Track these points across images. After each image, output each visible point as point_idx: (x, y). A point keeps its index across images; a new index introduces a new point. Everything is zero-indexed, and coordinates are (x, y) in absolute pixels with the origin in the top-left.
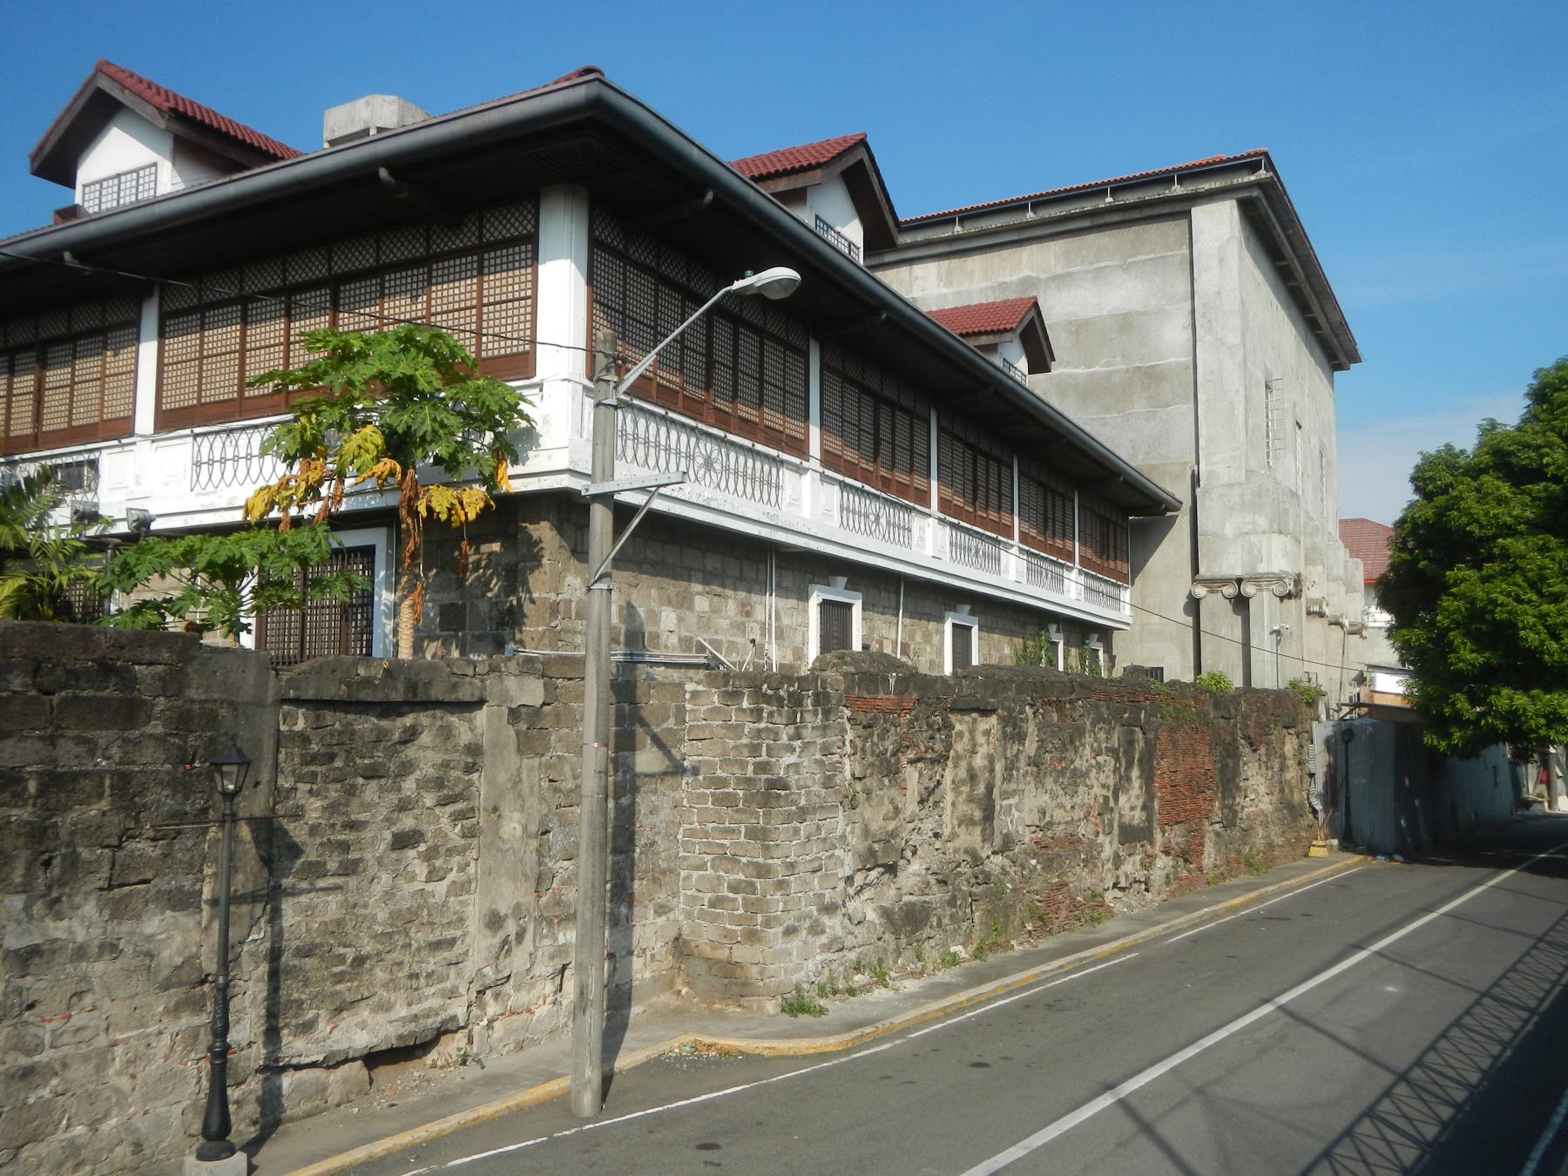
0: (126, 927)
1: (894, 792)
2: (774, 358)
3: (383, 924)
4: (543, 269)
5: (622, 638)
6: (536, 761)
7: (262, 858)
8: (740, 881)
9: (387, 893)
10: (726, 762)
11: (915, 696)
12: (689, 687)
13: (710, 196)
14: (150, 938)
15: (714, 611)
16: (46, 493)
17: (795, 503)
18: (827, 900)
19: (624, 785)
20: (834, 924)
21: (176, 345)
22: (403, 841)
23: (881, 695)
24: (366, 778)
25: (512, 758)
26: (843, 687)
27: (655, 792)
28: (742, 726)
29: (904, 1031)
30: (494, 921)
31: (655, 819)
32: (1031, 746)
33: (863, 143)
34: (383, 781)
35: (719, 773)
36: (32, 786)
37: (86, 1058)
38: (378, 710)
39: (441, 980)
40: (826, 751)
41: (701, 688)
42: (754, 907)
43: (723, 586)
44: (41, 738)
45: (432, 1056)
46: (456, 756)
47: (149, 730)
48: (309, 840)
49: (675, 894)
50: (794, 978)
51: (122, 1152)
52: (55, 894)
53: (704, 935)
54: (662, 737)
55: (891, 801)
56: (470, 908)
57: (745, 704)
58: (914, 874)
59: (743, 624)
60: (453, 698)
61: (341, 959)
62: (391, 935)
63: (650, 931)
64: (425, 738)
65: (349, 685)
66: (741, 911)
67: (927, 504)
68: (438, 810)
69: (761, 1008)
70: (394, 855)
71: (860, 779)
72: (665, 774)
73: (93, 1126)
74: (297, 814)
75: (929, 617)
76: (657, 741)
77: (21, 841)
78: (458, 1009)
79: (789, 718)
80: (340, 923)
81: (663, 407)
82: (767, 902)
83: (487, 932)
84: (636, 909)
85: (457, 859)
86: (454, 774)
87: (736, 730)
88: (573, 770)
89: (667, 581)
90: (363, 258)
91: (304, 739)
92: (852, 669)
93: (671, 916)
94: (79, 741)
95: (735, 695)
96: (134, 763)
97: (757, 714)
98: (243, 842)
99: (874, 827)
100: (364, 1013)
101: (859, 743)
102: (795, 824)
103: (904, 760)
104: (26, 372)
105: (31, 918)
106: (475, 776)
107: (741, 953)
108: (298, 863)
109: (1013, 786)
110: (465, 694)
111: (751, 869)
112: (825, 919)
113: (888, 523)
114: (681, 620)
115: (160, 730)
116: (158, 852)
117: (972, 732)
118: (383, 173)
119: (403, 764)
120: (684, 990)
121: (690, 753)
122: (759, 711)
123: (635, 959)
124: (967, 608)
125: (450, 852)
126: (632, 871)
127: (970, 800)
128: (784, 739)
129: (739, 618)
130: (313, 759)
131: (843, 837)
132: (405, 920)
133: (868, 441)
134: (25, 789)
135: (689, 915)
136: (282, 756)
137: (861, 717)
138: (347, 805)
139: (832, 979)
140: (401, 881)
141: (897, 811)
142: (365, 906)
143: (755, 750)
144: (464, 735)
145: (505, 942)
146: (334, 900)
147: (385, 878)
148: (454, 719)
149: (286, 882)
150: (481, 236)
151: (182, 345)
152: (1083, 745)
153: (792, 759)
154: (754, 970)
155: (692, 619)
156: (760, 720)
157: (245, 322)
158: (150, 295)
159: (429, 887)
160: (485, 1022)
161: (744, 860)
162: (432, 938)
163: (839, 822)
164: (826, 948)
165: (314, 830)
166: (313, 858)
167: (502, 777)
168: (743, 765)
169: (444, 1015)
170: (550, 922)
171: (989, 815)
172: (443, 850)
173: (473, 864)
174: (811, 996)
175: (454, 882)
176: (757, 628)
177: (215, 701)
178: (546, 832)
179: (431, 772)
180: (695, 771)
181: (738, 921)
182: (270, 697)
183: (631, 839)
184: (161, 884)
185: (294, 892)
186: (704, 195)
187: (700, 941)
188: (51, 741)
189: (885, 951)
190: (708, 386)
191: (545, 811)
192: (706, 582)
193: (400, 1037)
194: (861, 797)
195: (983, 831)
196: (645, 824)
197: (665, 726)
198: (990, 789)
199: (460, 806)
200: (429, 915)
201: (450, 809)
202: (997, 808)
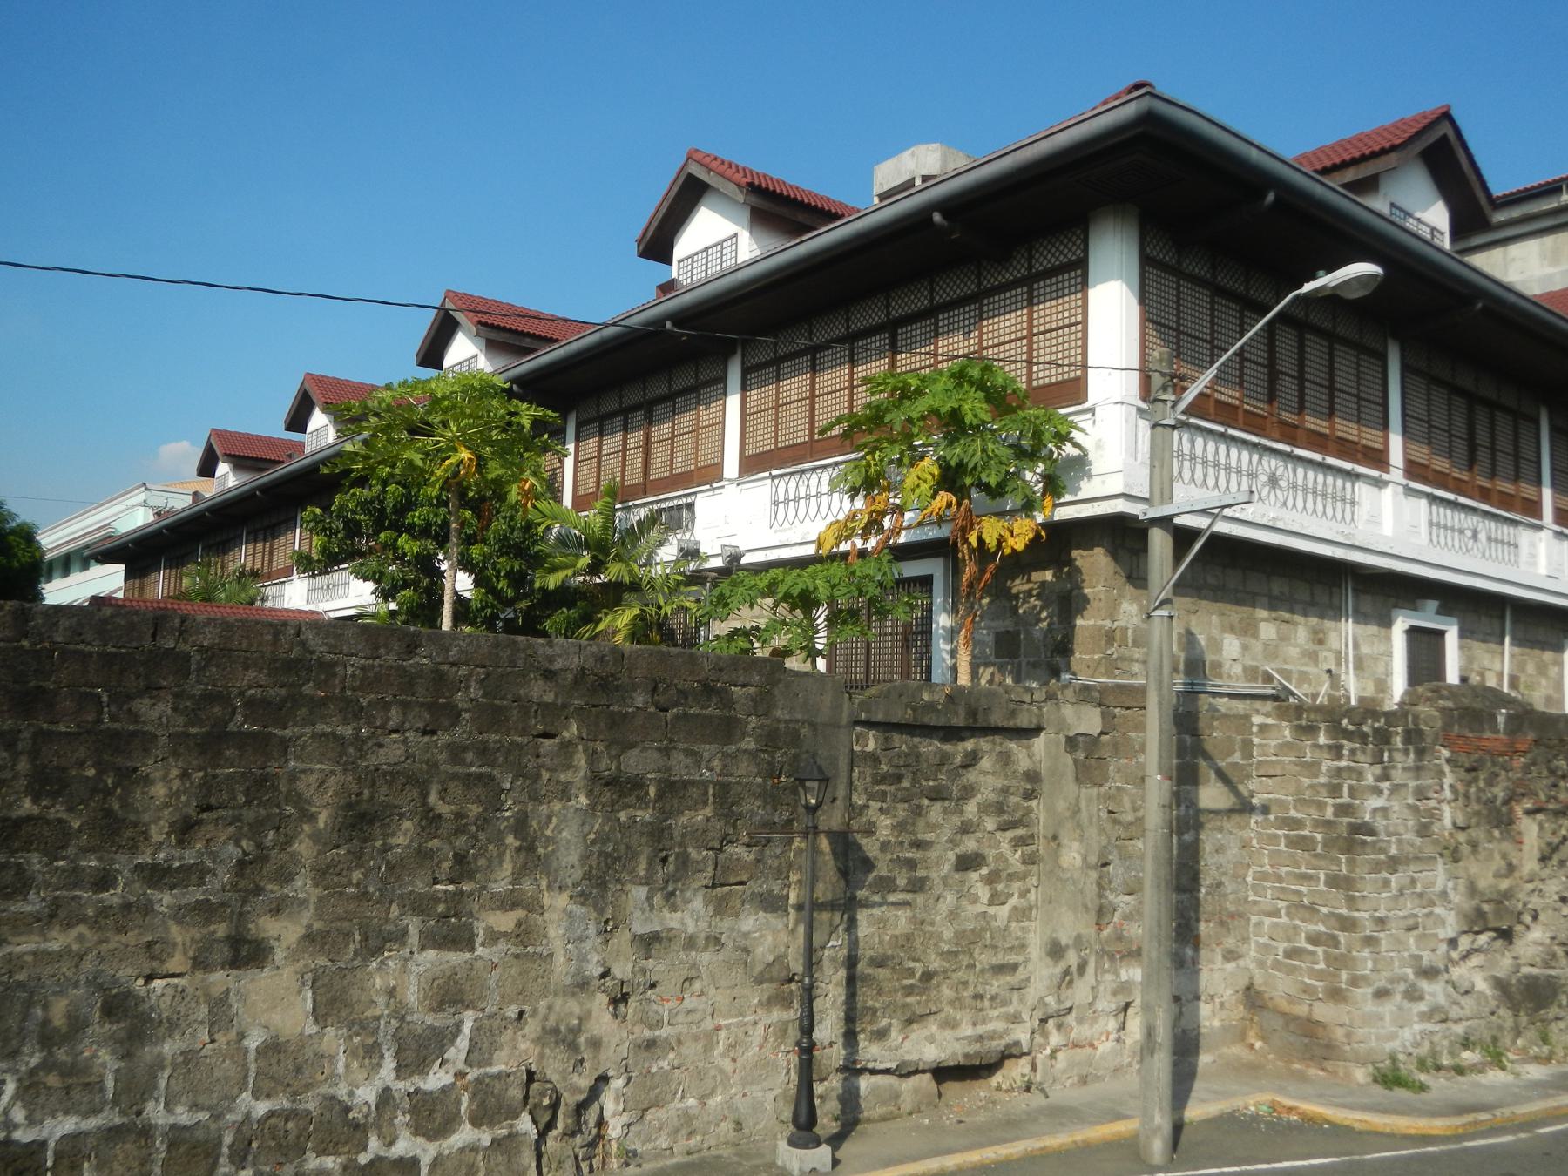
0: (726, 924)
2: (1345, 364)
3: (949, 942)
4: (1093, 294)
5: (1182, 667)
6: (1095, 791)
7: (839, 870)
8: (1319, 934)
9: (951, 912)
10: (1300, 802)
11: (1531, 736)
12: (1257, 720)
13: (1271, 197)
14: (746, 935)
16: (654, 534)
17: (1375, 519)
18: (1425, 962)
19: (1187, 822)
20: (1435, 991)
21: (756, 395)
22: (967, 863)
23: (1488, 734)
24: (932, 799)
25: (1070, 787)
26: (1439, 724)
27: (1221, 829)
28: (1319, 764)
29: (1530, 1124)
30: (1055, 951)
31: (1221, 859)
33: (1446, 116)
34: (947, 803)
35: (1293, 813)
36: (652, 791)
37: (696, 1038)
38: (941, 734)
39: (1005, 1003)
40: (1421, 794)
41: (1270, 721)
42: (1339, 962)
43: (1292, 612)
44: (659, 749)
45: (997, 1079)
46: (1015, 782)
47: (744, 745)
48: (880, 856)
49: (1245, 940)
50: (1389, 1046)
51: (726, 1127)
52: (670, 888)
53: (1280, 988)
54: (1229, 772)
55: (1504, 856)
56: (1032, 935)
57: (1322, 740)
58: (1536, 943)
60: (1011, 724)
61: (911, 973)
62: (956, 954)
63: (1218, 978)
64: (985, 763)
65: (914, 709)
66: (1322, 966)
67: (1540, 517)
68: (998, 835)
69: (1348, 1075)
70: (957, 876)
71: (1463, 829)
72: (1231, 811)
73: (702, 1100)
74: (870, 831)
75: (1544, 646)
76: (1222, 776)
77: (644, 840)
78: (1022, 1035)
79: (1374, 756)
80: (909, 937)
81: (1221, 424)
82: (1354, 959)
83: (1048, 960)
84: (1203, 953)
85: (1017, 885)
86: (1014, 800)
87: (1312, 768)
88: (1133, 802)
89: (1228, 606)
90: (918, 300)
91: (874, 759)
92: (1450, 704)
93: (1241, 963)
94: (689, 753)
95: (1310, 730)
96: (732, 775)
97: (1336, 752)
98: (822, 853)
99: (1482, 884)
100: (933, 1027)
101: (1460, 787)
102: (1385, 874)
103: (1518, 810)
104: (636, 429)
105: (652, 908)
106: (1034, 803)
107: (1324, 1012)
108: (872, 876)
110: (1023, 721)
111: (1333, 922)
112: (1424, 985)
113: (1489, 539)
114: (1245, 648)
115: (752, 746)
116: (752, 857)
118: (937, 217)
119: (965, 788)
120: (1258, 1044)
121: (1259, 790)
122: (1339, 748)
123: (1202, 1005)
125: (1012, 877)
126: (1197, 911)
128: (1369, 779)
129: (1311, 647)
130: (882, 779)
131: (1444, 894)
132: (969, 941)
133: (1461, 447)
134: (647, 793)
135: (1261, 964)
136: (855, 775)
137: (1464, 759)
138: (914, 824)
139: (1434, 1054)
140: (964, 903)
141: (1511, 868)
142: (932, 924)
143: (1335, 790)
144: (1023, 764)
145: (1067, 972)
146: (903, 915)
147: (950, 898)
148: (1013, 745)
149: (861, 894)
150: (1030, 267)
151: (762, 395)
153: (1375, 802)
154: (1339, 1034)
155: (1258, 647)
156: (1339, 757)
157: (814, 370)
158: (734, 353)
159: (992, 910)
160: (1048, 1051)
161: (1324, 910)
162: (994, 961)
163: (1439, 876)
164: (1426, 1017)
165: (885, 846)
166: (884, 873)
167: (1061, 805)
168: (1321, 806)
169: (1007, 1040)
170: (1112, 957)
172: (1004, 875)
173: (1033, 891)
174: (1408, 1068)
175: (1015, 908)
176: (1331, 656)
177: (797, 721)
178: (1106, 864)
179: (992, 797)
180: (1265, 810)
181: (1319, 975)
182: (845, 718)
183: (1195, 879)
184: (755, 886)
185: (868, 905)
186: (1264, 197)
187: (1274, 993)
188: (666, 752)
189: (1500, 1028)
190: (1271, 397)
191: (1104, 842)
192: (1272, 608)
193: (966, 1056)
194: (1465, 849)
196: (1210, 863)
197: (1230, 760)
199: (1020, 832)
200: (992, 938)
201: (1010, 834)
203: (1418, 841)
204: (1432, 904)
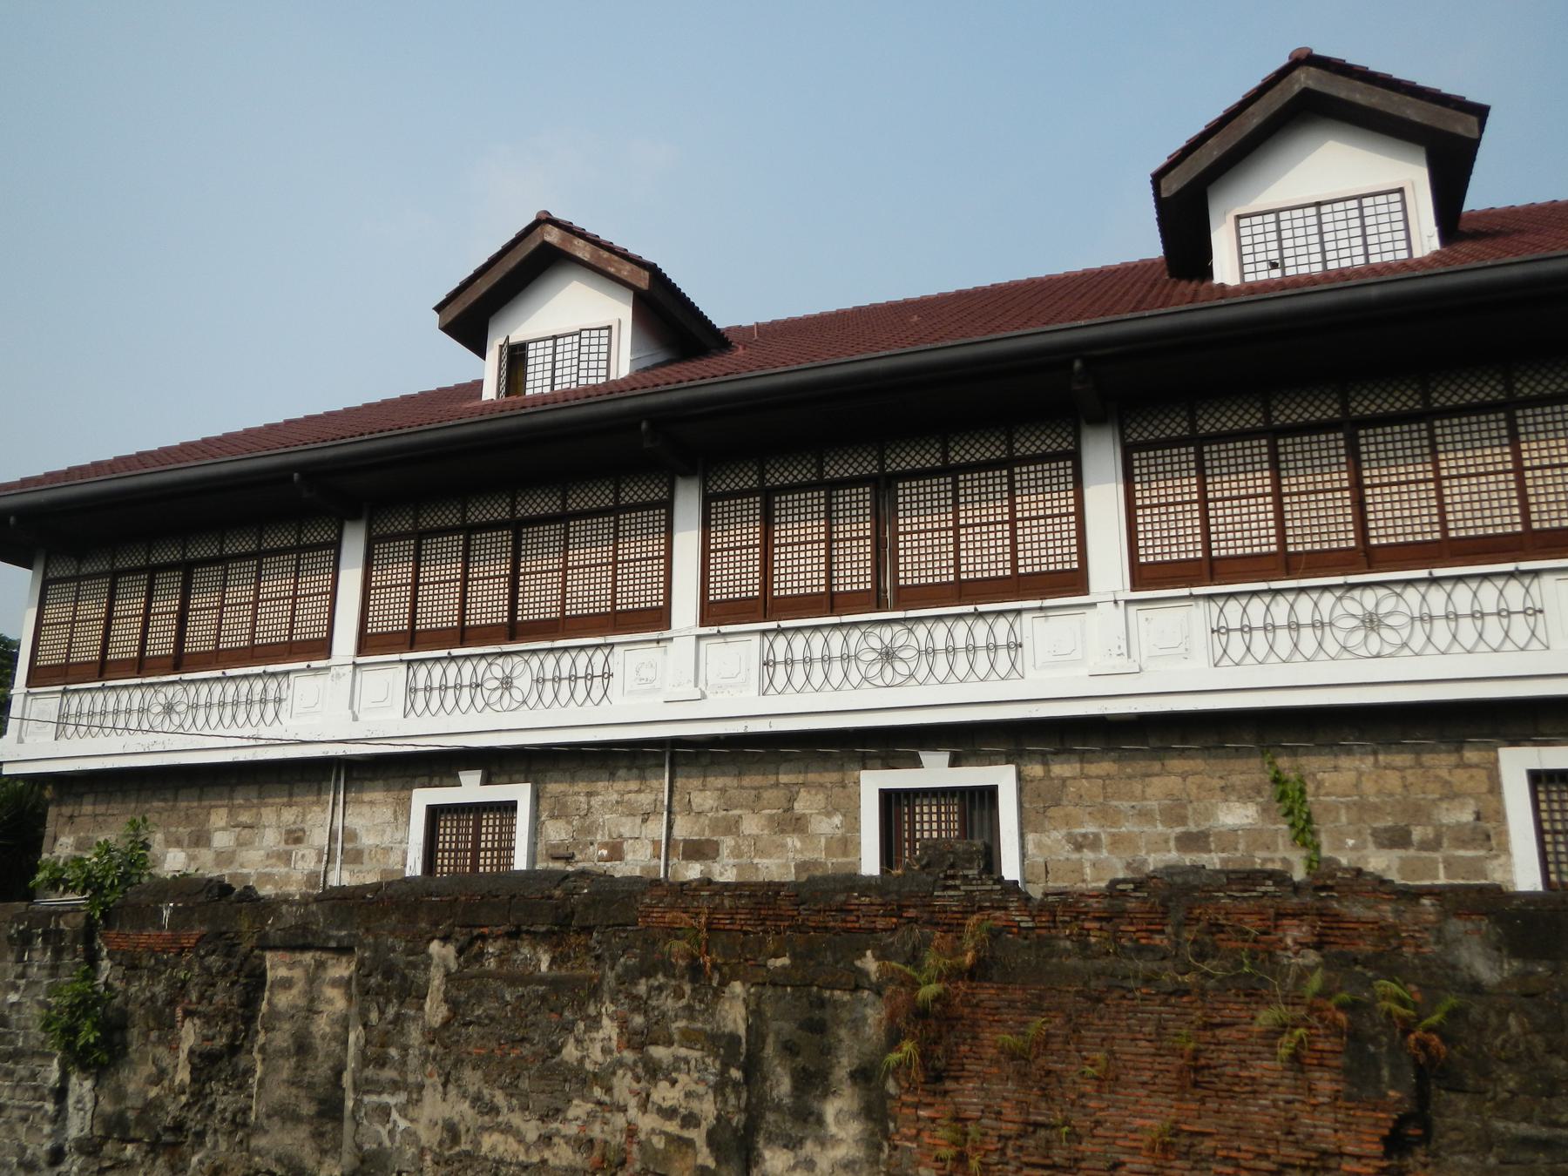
1: (161, 1051)
15: (241, 844)
32: (435, 1011)
59: (289, 854)
103: (179, 1013)
109: (389, 1074)
117: (312, 980)
124: (944, 757)
127: (293, 1083)
129: (282, 846)
141: (162, 1073)
152: (594, 1023)
171: (330, 1109)
195: (318, 1135)
198: (338, 1072)
202: (349, 1104)
203: (42, 1036)
204: (42, 1098)
